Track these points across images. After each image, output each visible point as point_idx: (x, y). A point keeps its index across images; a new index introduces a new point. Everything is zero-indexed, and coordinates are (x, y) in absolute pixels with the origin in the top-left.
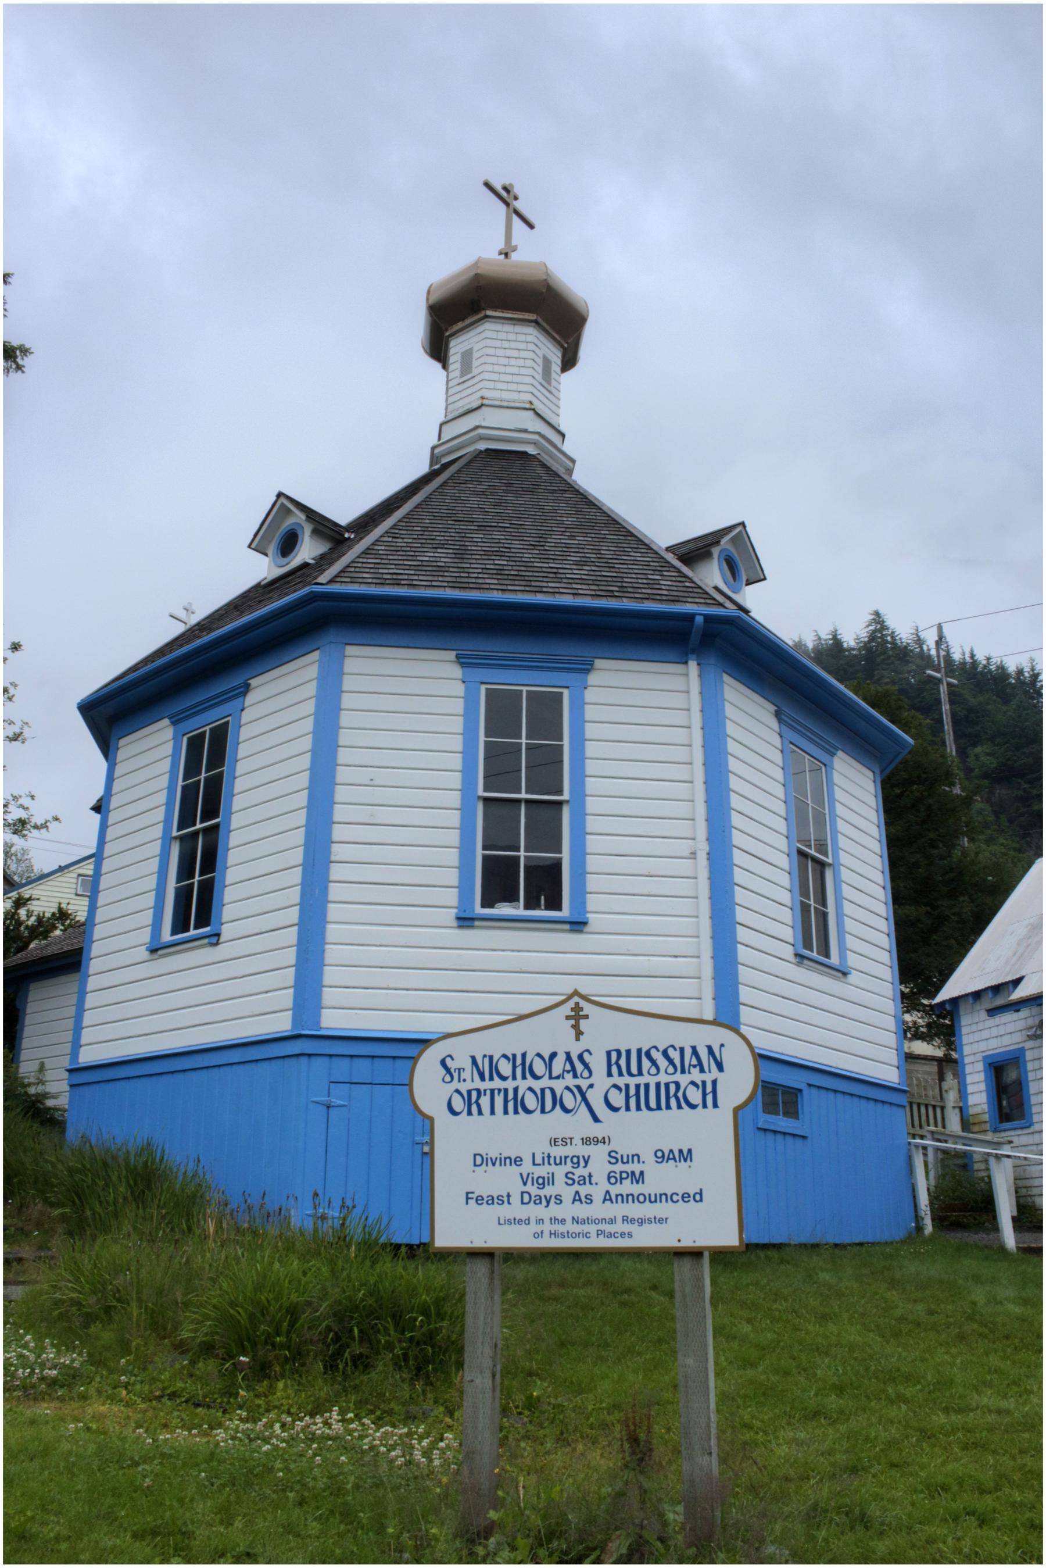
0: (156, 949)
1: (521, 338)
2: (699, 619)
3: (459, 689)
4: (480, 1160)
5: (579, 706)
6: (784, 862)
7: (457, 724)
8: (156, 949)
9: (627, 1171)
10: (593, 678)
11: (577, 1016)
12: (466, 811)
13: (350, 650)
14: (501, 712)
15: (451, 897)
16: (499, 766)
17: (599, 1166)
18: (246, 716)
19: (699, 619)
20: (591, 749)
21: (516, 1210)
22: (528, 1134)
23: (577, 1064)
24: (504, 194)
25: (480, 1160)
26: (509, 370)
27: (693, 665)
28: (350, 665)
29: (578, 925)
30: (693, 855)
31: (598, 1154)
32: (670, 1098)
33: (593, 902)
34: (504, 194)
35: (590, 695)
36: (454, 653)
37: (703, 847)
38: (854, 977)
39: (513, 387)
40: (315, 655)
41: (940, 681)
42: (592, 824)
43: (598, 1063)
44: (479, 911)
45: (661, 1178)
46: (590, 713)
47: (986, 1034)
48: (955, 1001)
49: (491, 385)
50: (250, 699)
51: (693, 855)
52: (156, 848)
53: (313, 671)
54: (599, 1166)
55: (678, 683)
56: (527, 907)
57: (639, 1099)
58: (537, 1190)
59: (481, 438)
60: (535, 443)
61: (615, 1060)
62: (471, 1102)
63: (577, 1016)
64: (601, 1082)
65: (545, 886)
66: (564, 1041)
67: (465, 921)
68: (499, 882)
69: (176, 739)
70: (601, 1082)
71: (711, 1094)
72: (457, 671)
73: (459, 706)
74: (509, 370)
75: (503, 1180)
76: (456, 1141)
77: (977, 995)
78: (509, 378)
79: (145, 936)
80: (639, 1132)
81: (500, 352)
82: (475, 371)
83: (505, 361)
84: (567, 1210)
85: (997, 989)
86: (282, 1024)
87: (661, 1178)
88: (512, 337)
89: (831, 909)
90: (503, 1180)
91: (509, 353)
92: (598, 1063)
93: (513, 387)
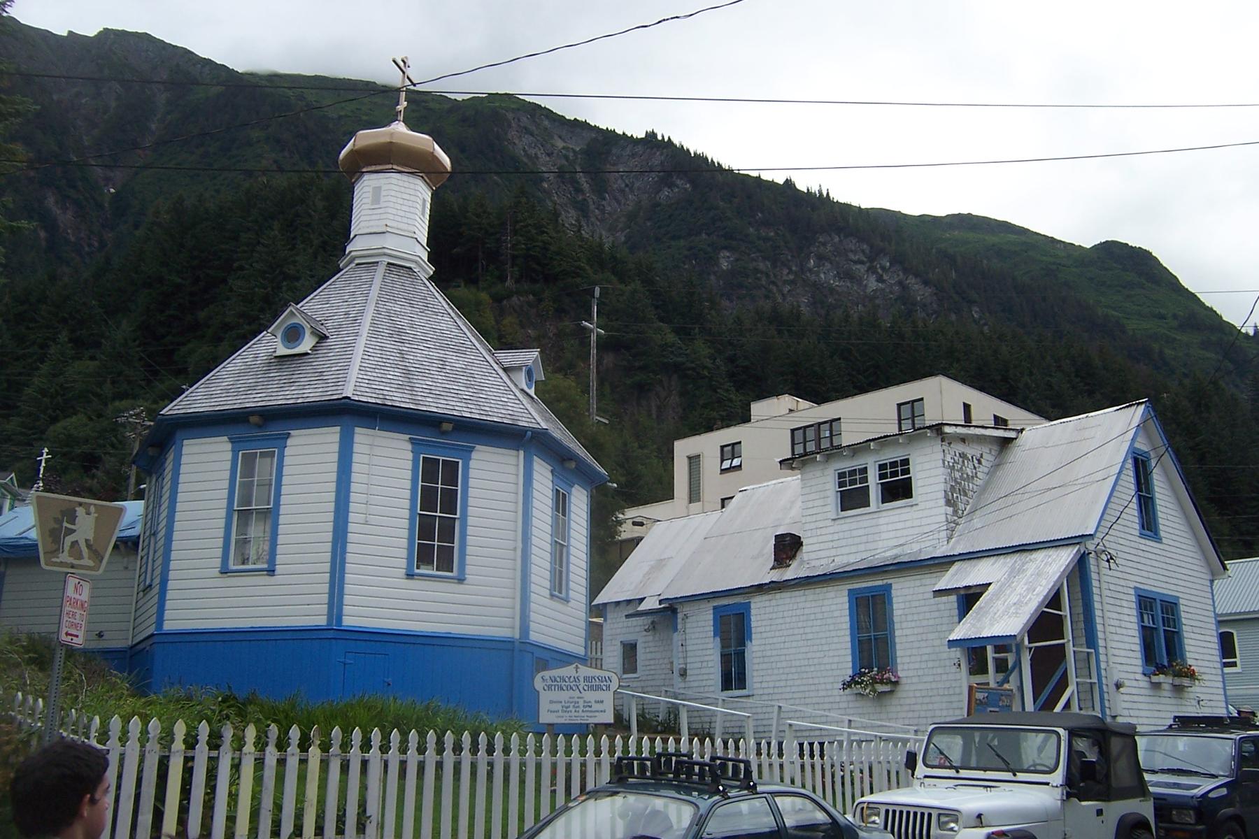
0: (225, 571)
1: (412, 186)
2: (529, 433)
3: (410, 456)
4: (551, 702)
5: (466, 468)
6: (548, 548)
7: (409, 474)
8: (225, 571)
9: (588, 705)
10: (474, 455)
11: (577, 667)
12: (411, 519)
13: (357, 430)
14: (429, 469)
15: (404, 563)
16: (428, 499)
17: (581, 704)
18: (287, 451)
19: (529, 433)
20: (471, 492)
21: (560, 714)
22: (564, 696)
23: (577, 679)
24: (402, 64)
25: (551, 702)
26: (404, 208)
27: (522, 453)
28: (357, 438)
29: (461, 580)
30: (515, 549)
31: (581, 701)
32: (599, 688)
33: (468, 569)
34: (402, 64)
35: (472, 464)
36: (408, 437)
37: (520, 545)
38: (572, 603)
39: (405, 220)
40: (338, 428)
41: (591, 331)
42: (470, 530)
43: (582, 679)
44: (417, 571)
45: (596, 707)
46: (472, 473)
47: (620, 625)
48: (605, 605)
49: (391, 217)
50: (289, 442)
51: (515, 549)
52: (223, 513)
53: (337, 438)
54: (581, 704)
55: (512, 460)
56: (438, 570)
57: (591, 688)
58: (566, 709)
59: (385, 254)
60: (416, 262)
61: (585, 679)
62: (549, 687)
63: (577, 667)
64: (582, 683)
65: (446, 561)
66: (573, 673)
67: (410, 576)
68: (424, 556)
69: (235, 453)
70: (582, 683)
71: (608, 688)
72: (409, 447)
73: (409, 465)
74: (404, 208)
75: (558, 707)
76: (545, 698)
77: (618, 603)
78: (402, 214)
79: (218, 562)
80: (591, 696)
81: (399, 195)
82: (383, 205)
83: (401, 201)
84: (573, 714)
85: (629, 602)
86: (322, 621)
87: (596, 707)
88: (406, 184)
89: (564, 570)
90: (558, 707)
91: (405, 196)
92: (582, 679)
93: (405, 220)
